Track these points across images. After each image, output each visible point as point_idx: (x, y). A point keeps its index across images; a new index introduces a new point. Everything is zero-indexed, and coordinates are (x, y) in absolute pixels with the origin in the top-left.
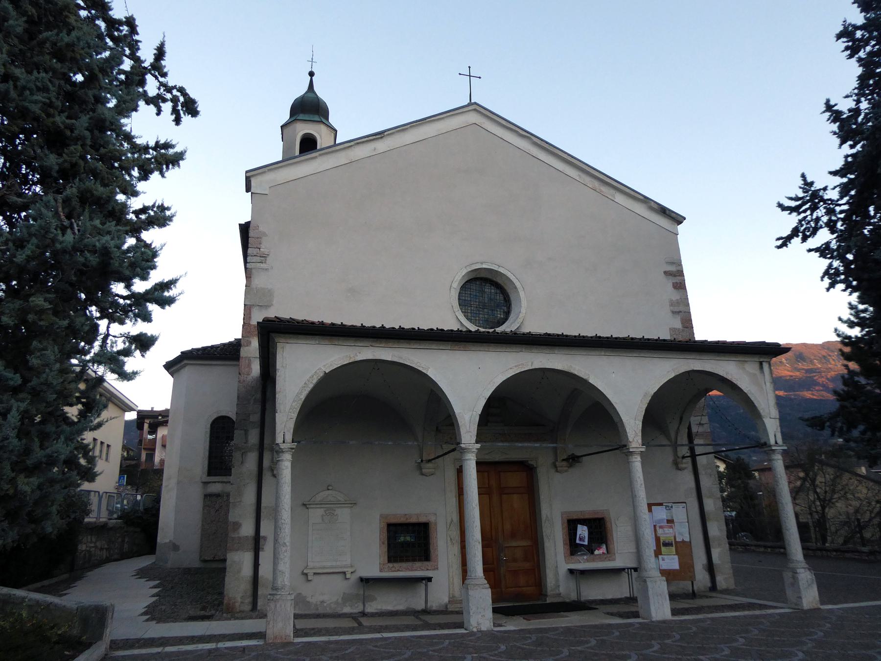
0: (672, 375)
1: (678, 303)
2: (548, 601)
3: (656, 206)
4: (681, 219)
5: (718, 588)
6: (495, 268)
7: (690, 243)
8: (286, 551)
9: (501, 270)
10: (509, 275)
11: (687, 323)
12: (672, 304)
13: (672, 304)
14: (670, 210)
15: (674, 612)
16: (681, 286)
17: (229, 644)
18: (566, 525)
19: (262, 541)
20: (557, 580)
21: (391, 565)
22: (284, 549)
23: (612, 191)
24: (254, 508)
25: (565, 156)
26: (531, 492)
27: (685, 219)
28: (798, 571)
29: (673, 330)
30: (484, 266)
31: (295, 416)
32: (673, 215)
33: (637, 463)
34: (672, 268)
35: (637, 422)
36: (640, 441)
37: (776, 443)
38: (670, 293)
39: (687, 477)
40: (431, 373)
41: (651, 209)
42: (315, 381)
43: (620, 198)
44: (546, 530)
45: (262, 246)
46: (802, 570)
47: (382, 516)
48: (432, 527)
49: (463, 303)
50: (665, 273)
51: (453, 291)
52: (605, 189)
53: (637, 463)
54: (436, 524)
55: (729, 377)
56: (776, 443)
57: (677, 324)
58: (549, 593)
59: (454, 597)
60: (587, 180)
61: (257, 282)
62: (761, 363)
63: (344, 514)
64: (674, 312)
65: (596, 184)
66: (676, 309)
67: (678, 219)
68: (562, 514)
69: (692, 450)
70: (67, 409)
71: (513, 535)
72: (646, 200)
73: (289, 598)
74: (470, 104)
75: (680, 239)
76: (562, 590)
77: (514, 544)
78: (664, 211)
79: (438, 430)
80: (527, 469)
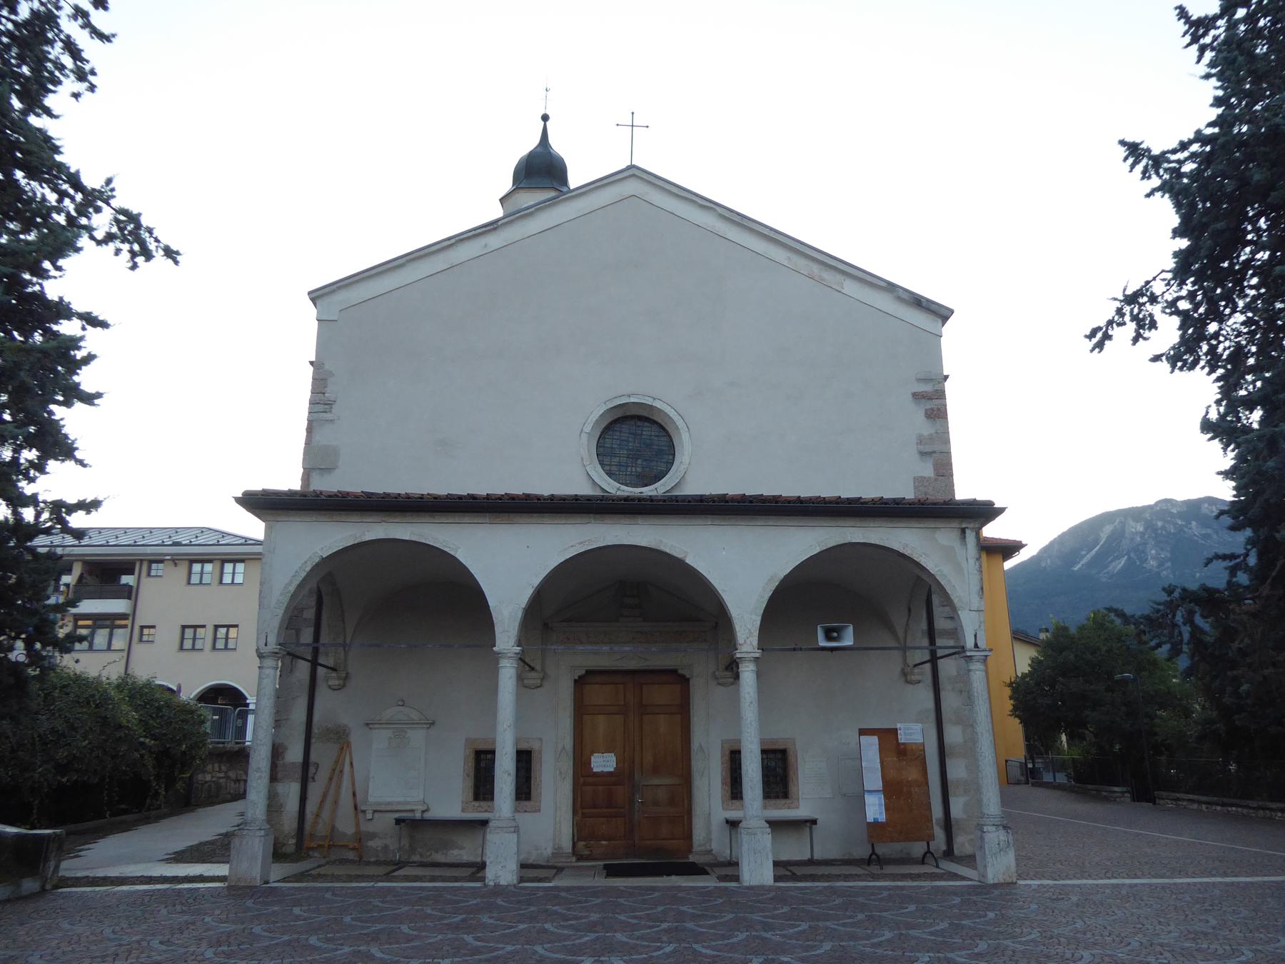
0: (817, 550)
1: (931, 439)
2: (692, 858)
3: (905, 296)
4: (945, 313)
5: (956, 852)
6: (649, 401)
7: (955, 346)
8: (260, 778)
9: (658, 404)
10: (672, 414)
11: (944, 468)
12: (921, 440)
13: (921, 440)
14: (928, 300)
15: (777, 878)
16: (938, 414)
17: (186, 886)
18: (727, 758)
19: (312, 770)
20: (709, 833)
21: (477, 804)
22: (258, 775)
23: (839, 277)
24: (303, 728)
25: (766, 232)
26: (683, 710)
27: (952, 312)
28: (985, 829)
29: (919, 481)
30: (632, 400)
31: (280, 612)
32: (933, 307)
33: (748, 674)
34: (927, 388)
35: (754, 617)
36: (755, 643)
37: (976, 646)
38: (919, 423)
39: (924, 696)
40: (461, 556)
41: (899, 299)
42: (308, 569)
43: (850, 287)
44: (697, 764)
45: (328, 390)
46: (990, 828)
47: (469, 741)
48: (534, 756)
49: (604, 453)
50: (915, 395)
51: (584, 436)
52: (828, 276)
53: (507, 673)
54: (540, 752)
55: (907, 552)
56: (976, 646)
57: (927, 470)
58: (696, 848)
59: (560, 848)
60: (801, 263)
61: (317, 437)
62: (963, 531)
63: (417, 737)
64: (922, 454)
65: (815, 268)
66: (928, 449)
67: (943, 314)
68: (723, 742)
69: (933, 653)
70: (47, 602)
71: (656, 770)
72: (891, 288)
73: (258, 833)
74: (629, 168)
75: (944, 342)
76: (715, 846)
77: (656, 781)
78: (919, 303)
79: (546, 625)
80: (679, 680)
